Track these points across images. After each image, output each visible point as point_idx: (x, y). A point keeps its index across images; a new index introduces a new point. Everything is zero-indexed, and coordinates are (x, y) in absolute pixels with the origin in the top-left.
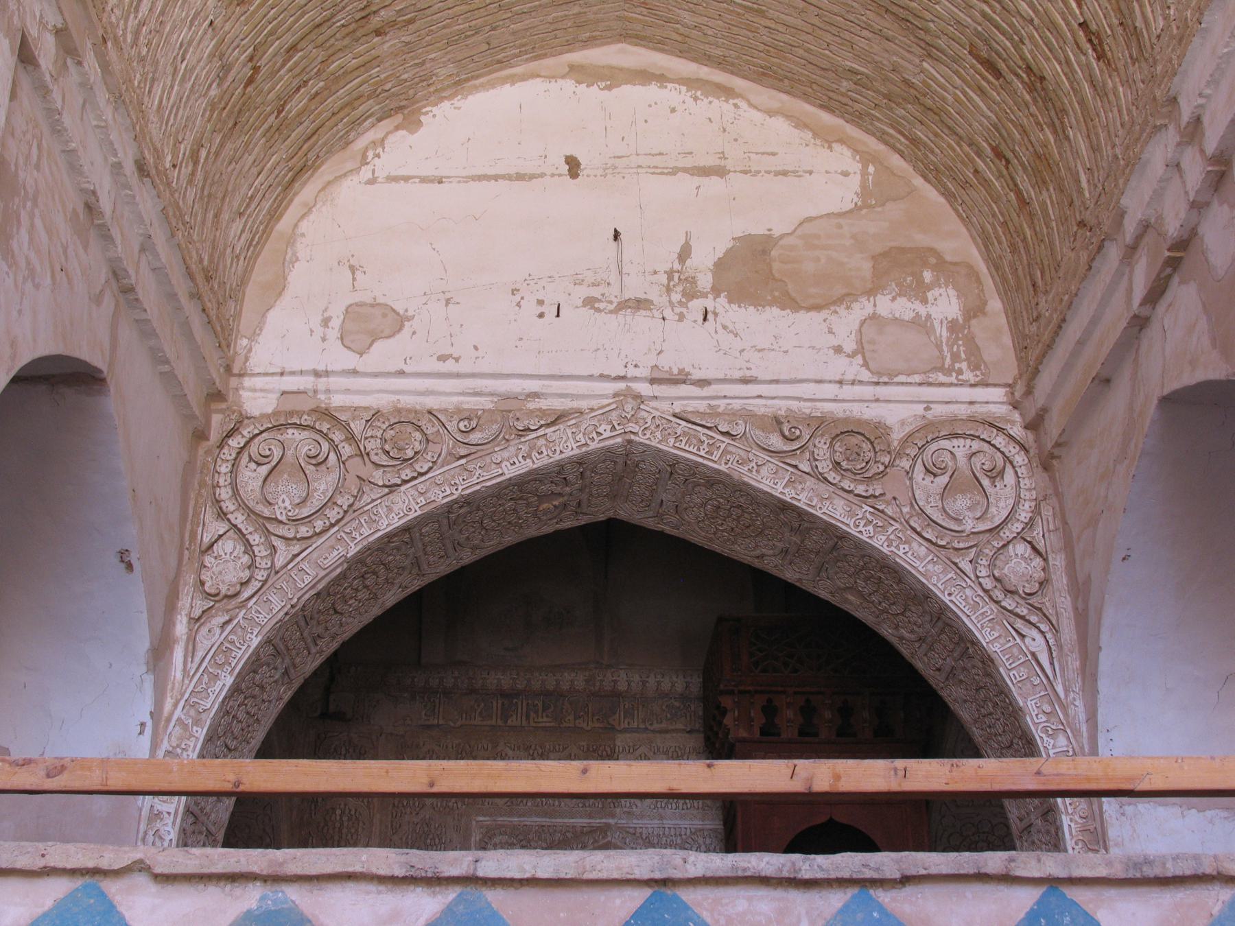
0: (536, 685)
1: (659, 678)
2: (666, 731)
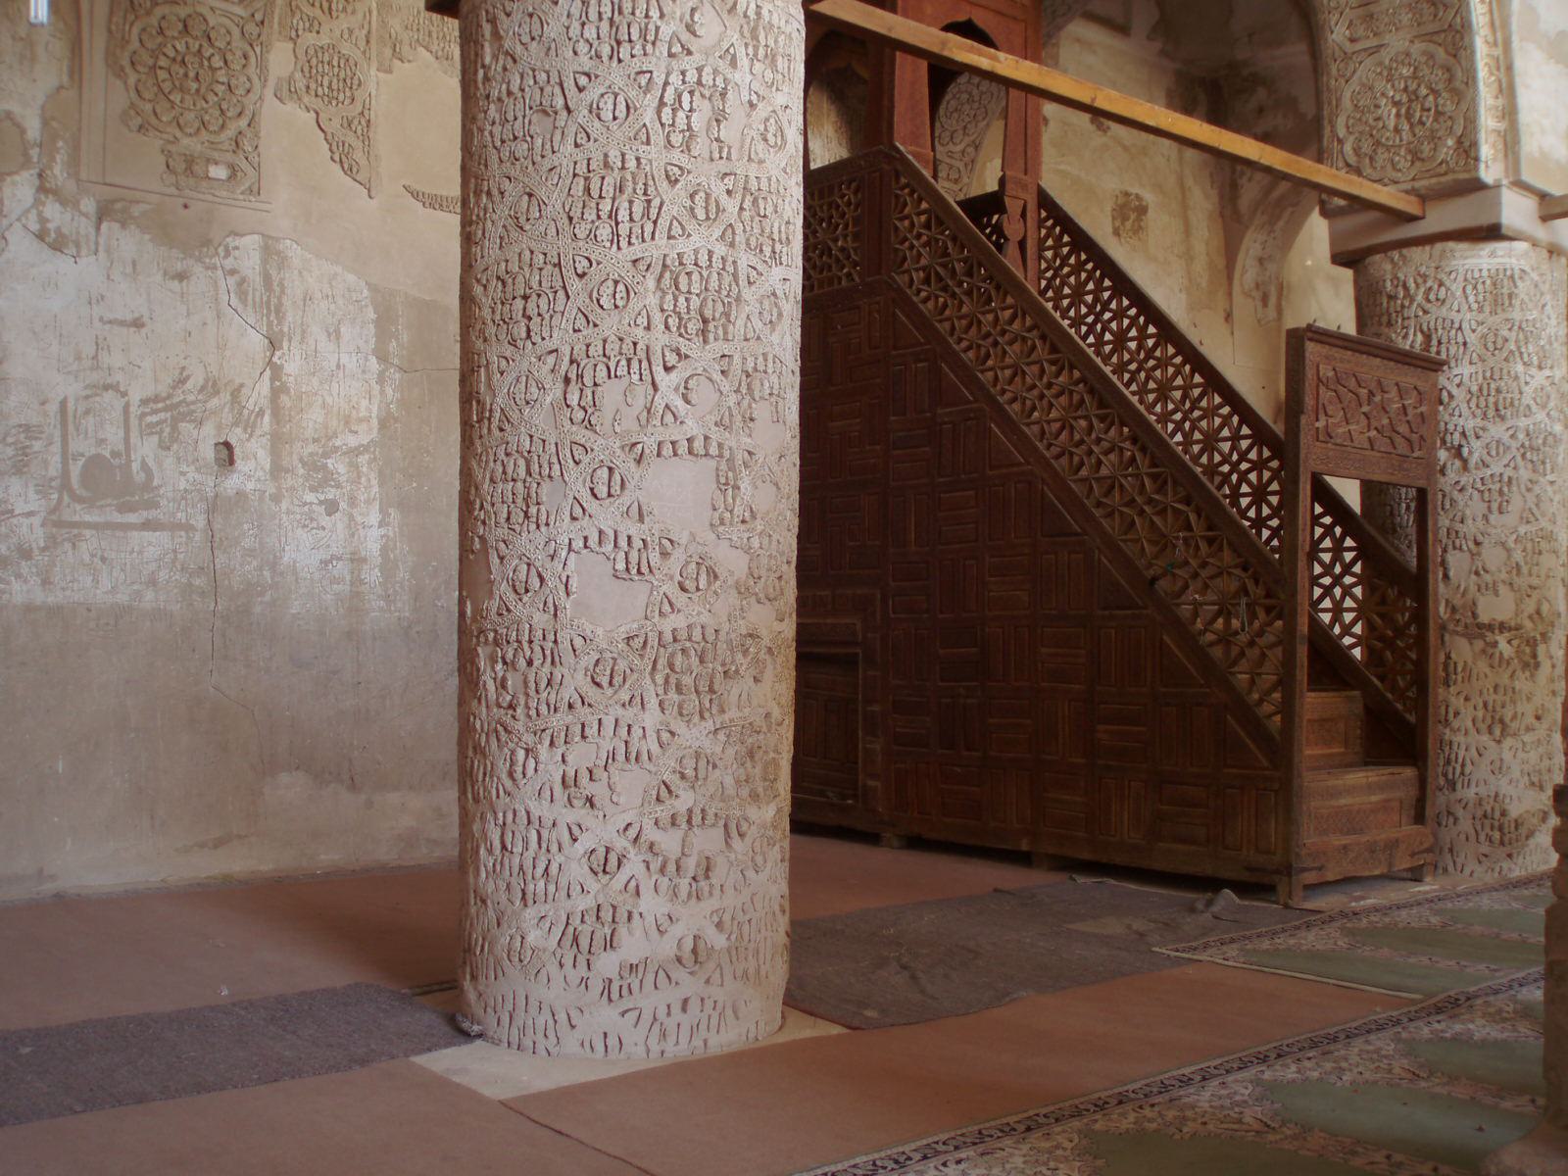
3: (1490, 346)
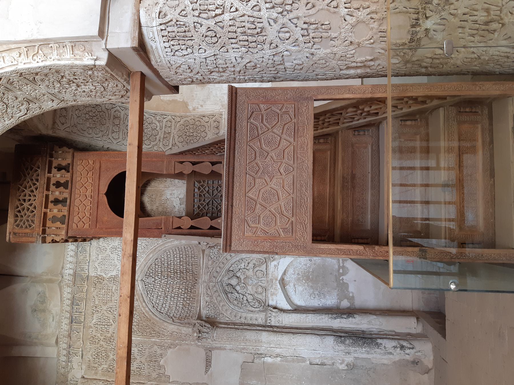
0: (68, 309)
1: (69, 256)
2: (90, 254)
3: (215, 40)
